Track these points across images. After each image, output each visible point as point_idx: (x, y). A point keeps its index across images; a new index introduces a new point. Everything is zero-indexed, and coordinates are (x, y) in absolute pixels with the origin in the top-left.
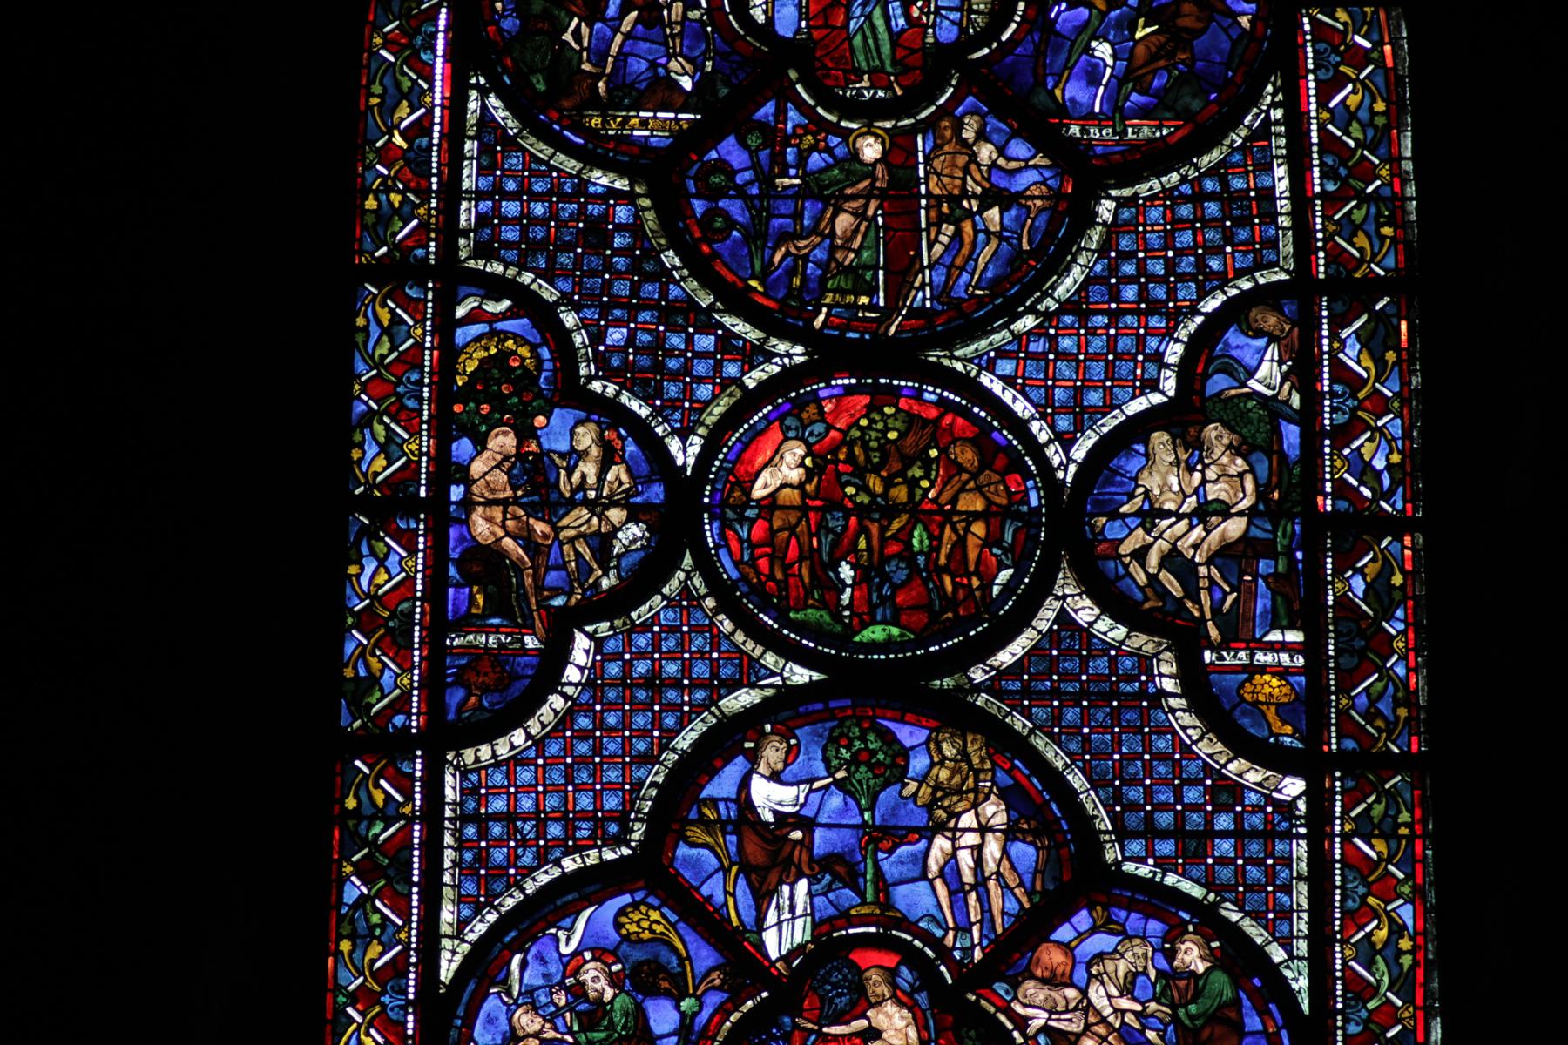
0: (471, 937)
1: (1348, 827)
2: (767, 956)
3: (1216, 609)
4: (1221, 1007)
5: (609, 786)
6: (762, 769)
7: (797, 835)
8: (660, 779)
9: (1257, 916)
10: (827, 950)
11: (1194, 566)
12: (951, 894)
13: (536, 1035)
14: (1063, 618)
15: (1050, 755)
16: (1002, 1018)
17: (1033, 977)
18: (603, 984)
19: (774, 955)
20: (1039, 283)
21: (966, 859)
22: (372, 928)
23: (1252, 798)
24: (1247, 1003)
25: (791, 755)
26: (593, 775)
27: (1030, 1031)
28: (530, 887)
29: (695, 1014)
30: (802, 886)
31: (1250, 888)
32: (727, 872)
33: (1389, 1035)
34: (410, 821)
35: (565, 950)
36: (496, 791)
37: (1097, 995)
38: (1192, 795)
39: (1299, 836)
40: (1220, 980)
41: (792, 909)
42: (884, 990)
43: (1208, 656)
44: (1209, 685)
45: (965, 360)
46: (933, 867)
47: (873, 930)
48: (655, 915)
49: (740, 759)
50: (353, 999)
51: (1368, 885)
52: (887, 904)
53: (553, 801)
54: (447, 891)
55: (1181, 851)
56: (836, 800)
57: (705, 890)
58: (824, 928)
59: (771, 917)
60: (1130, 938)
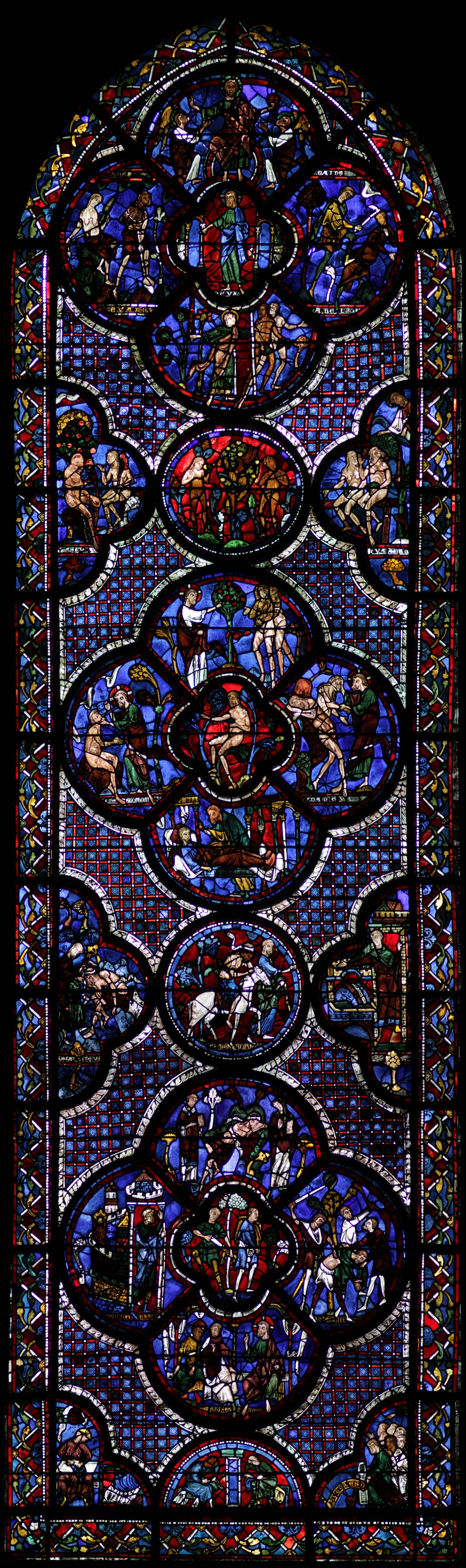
0: (72, 680)
3: (373, 530)
5: (125, 613)
11: (364, 511)
13: (99, 723)
14: (310, 536)
18: (124, 700)
20: (301, 384)
22: (33, 676)
23: (385, 613)
25: (199, 597)
28: (95, 658)
34: (46, 629)
35: (109, 686)
36: (80, 616)
43: (369, 551)
44: (369, 564)
45: (271, 419)
48: (144, 669)
53: (103, 620)
54: (62, 659)
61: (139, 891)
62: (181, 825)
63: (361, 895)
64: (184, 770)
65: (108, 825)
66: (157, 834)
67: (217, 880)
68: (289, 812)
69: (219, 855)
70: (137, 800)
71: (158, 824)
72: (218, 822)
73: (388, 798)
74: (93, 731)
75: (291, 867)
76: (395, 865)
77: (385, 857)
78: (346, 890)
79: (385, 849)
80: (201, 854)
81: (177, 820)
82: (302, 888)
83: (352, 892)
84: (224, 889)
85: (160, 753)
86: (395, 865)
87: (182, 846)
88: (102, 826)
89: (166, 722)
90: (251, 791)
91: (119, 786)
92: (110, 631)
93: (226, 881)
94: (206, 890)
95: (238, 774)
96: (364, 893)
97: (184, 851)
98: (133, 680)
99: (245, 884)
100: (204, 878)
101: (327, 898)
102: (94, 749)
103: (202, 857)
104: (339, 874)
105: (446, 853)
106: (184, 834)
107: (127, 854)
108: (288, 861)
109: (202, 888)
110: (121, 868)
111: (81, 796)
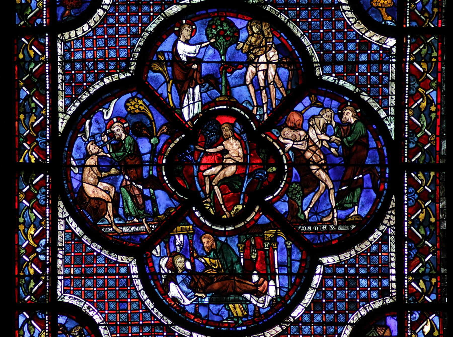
0: (70, 112)
1: (412, 59)
2: (184, 119)
4: (360, 137)
5: (122, 47)
6: (182, 39)
7: (195, 66)
8: (142, 44)
9: (375, 98)
10: (207, 116)
12: (255, 91)
13: (96, 154)
15: (295, 31)
16: (275, 144)
17: (287, 126)
18: (121, 132)
19: (187, 119)
21: (261, 75)
22: (32, 109)
24: (370, 135)
26: (115, 43)
27: (286, 149)
28: (92, 91)
29: (157, 145)
30: (197, 88)
31: (372, 86)
32: (168, 83)
33: (426, 148)
34: (45, 63)
35: (106, 118)
36: (78, 50)
37: (312, 134)
38: (351, 46)
39: (392, 63)
40: (360, 127)
41: (194, 99)
42: (229, 133)
46: (248, 79)
47: (225, 107)
48: (140, 102)
49: (173, 35)
50: (26, 139)
51: (419, 83)
52: (230, 96)
53: (100, 54)
54: (60, 92)
55: (346, 70)
56: (211, 51)
57: (160, 91)
58: (206, 107)
59: (185, 103)
60: (325, 109)
61: (136, 317)
62: (176, 253)
63: (351, 321)
64: (179, 200)
65: (105, 253)
66: (152, 261)
67: (211, 306)
68: (281, 240)
69: (213, 282)
70: (134, 228)
71: (154, 252)
72: (212, 250)
73: (377, 227)
74: (91, 161)
75: (283, 294)
76: (384, 292)
77: (374, 284)
78: (336, 316)
79: (374, 276)
80: (195, 280)
81: (172, 249)
82: (293, 314)
83: (342, 318)
84: (218, 315)
85: (155, 183)
86: (384, 292)
87: (176, 273)
88: (99, 254)
89: (161, 153)
90: (244, 220)
91: (116, 215)
92: (107, 65)
93: (220, 307)
94: (200, 316)
95: (231, 203)
96: (354, 319)
97: (179, 279)
98: (129, 112)
99: (238, 310)
100: (198, 304)
101: (318, 324)
102: (91, 180)
103: (196, 284)
104: (329, 300)
105: (434, 281)
106: (179, 261)
107: (123, 281)
108: (280, 288)
109: (196, 314)
110: (117, 295)
111: (79, 225)
